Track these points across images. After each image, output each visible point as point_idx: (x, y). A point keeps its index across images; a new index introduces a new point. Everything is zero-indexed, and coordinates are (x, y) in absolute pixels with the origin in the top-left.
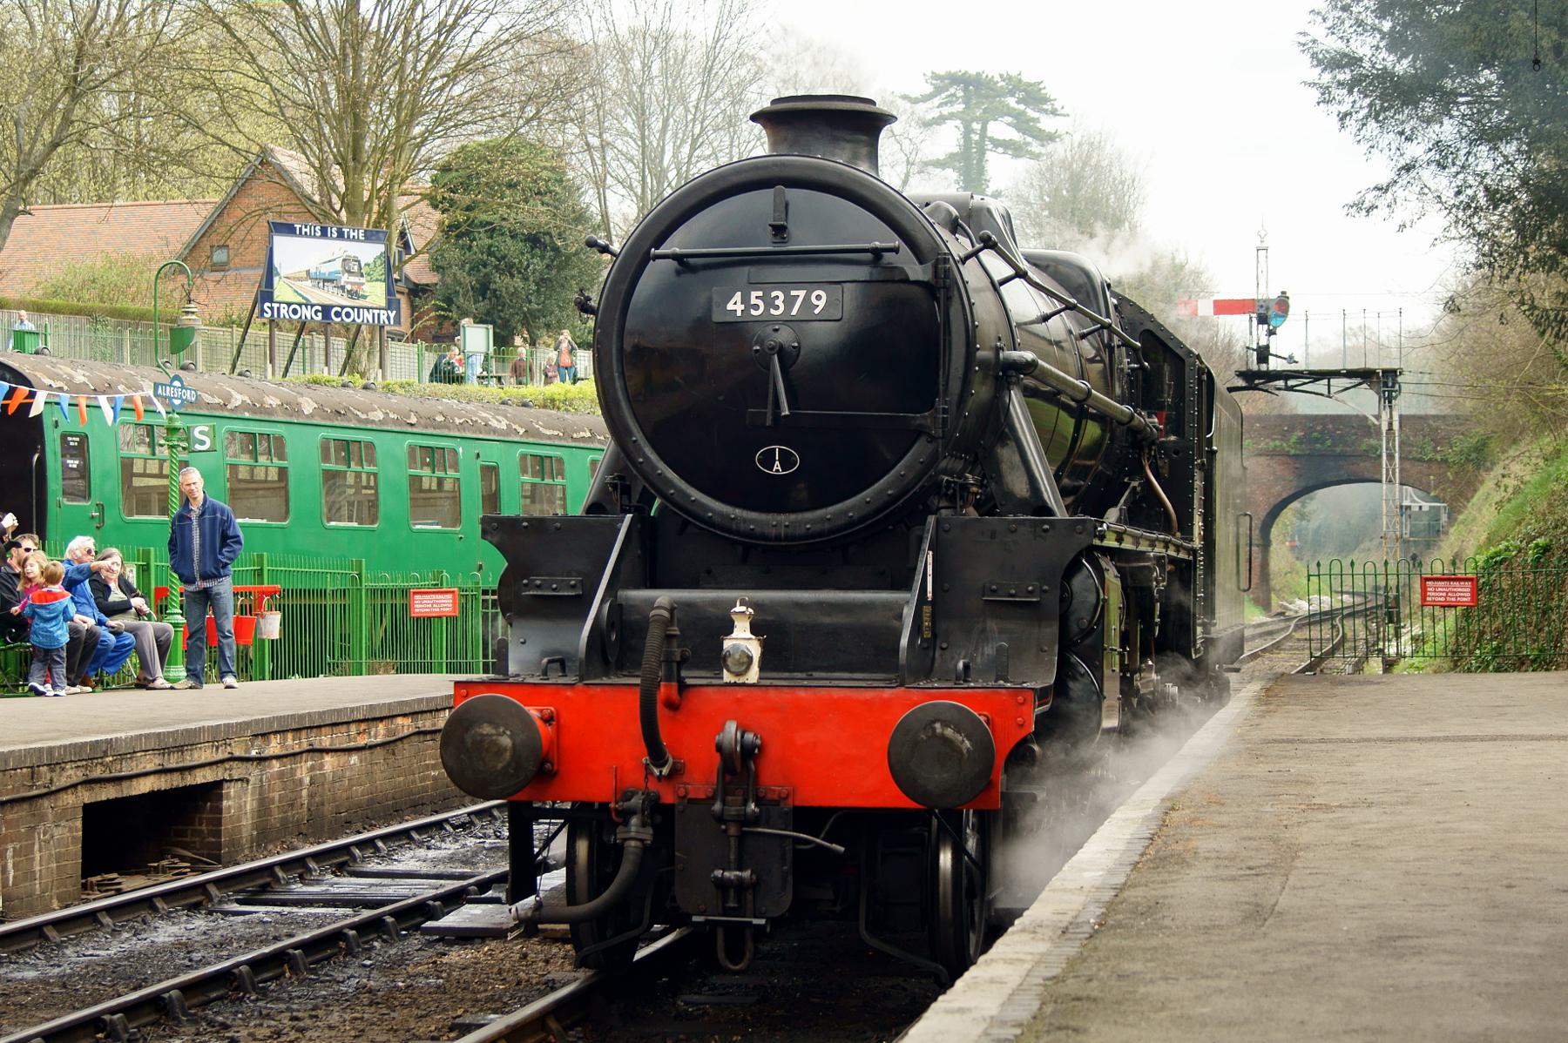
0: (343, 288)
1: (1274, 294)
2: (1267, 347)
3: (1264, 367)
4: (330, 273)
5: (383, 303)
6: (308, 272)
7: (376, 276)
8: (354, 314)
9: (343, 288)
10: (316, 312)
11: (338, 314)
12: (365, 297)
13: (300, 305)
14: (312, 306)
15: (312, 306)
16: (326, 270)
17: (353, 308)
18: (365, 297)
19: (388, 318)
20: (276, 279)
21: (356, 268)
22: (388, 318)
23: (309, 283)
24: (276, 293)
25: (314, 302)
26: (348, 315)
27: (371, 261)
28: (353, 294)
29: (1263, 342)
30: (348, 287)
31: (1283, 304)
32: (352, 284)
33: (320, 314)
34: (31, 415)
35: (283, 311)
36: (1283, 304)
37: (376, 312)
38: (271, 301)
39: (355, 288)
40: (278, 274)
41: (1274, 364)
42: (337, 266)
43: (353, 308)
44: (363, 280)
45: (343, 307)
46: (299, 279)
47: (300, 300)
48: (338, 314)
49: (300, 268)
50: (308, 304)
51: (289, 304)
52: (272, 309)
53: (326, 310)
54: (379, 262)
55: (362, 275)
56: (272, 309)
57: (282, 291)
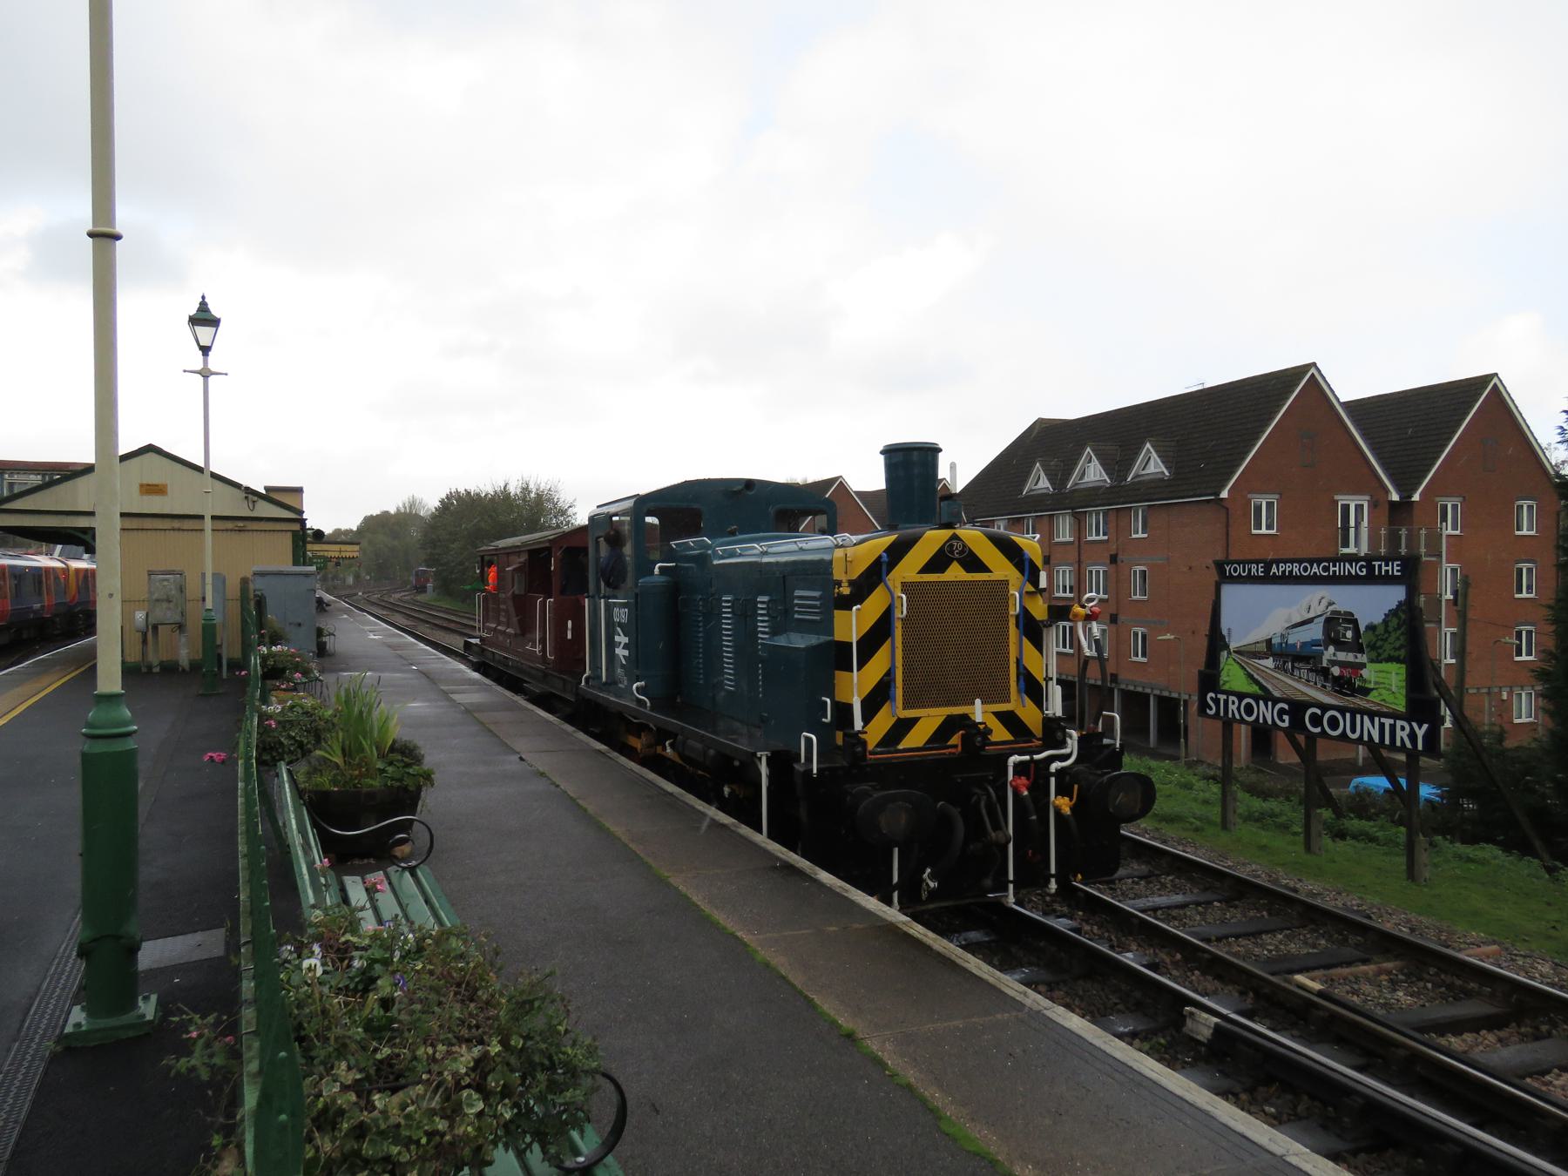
0: (1325, 672)
4: (1304, 644)
6: (1269, 642)
7: (1388, 649)
8: (1345, 723)
9: (1325, 672)
10: (1281, 712)
11: (1316, 721)
13: (1257, 698)
14: (1276, 701)
15: (1276, 701)
16: (1298, 637)
17: (1343, 711)
18: (1365, 692)
19: (1413, 736)
21: (1349, 634)
22: (1413, 736)
23: (1269, 663)
24: (1224, 677)
25: (1277, 694)
26: (1334, 723)
27: (1378, 619)
30: (1336, 671)
32: (1343, 665)
33: (1286, 717)
34: (727, 796)
35: (1233, 708)
37: (1388, 722)
39: (1346, 673)
40: (1227, 647)
42: (1316, 632)
43: (1343, 711)
44: (1362, 658)
45: (1325, 708)
47: (1255, 689)
50: (1267, 697)
51: (1241, 696)
52: (1216, 701)
53: (1297, 708)
54: (1394, 622)
55: (1361, 651)
56: (1216, 701)
57: (1233, 676)
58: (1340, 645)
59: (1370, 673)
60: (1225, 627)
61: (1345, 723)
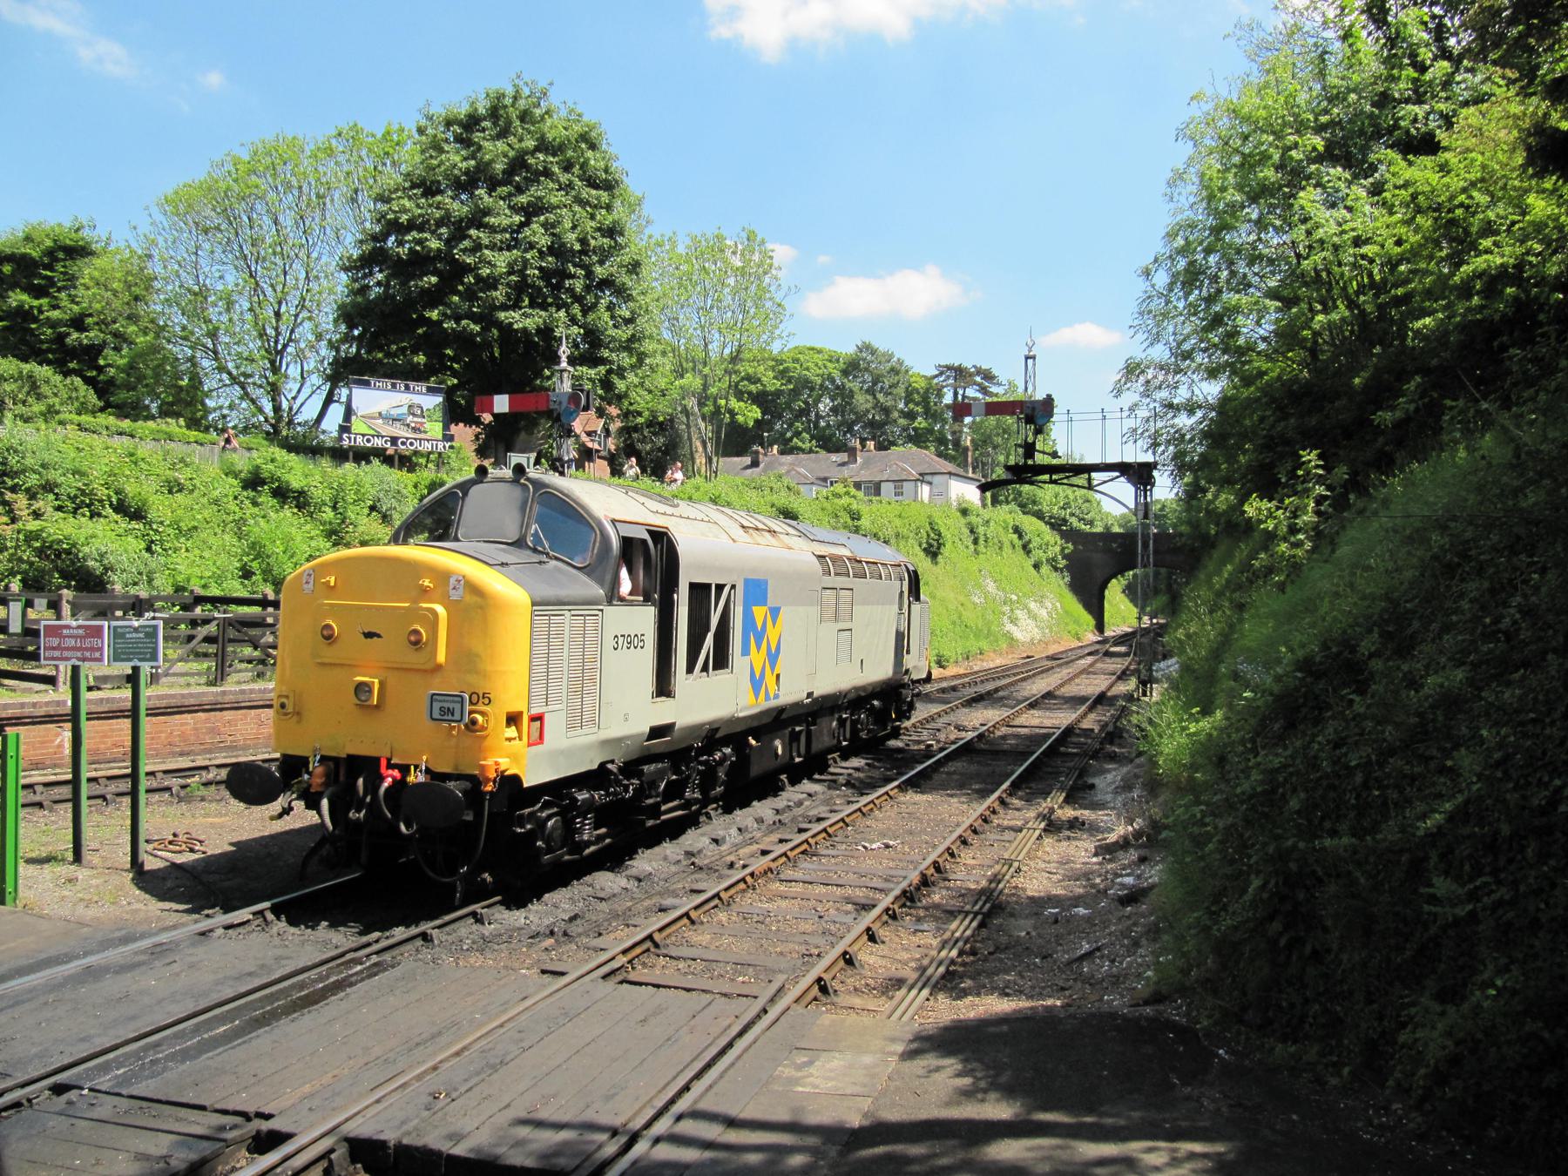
0: (408, 425)
1: (1040, 396)
2: (1034, 443)
3: (1030, 462)
5: (440, 437)
6: (380, 414)
8: (416, 444)
9: (408, 425)
12: (425, 432)
16: (395, 412)
18: (425, 432)
20: (353, 418)
23: (380, 421)
26: (411, 444)
28: (415, 430)
29: (1030, 439)
31: (1048, 404)
36: (1048, 404)
38: (349, 432)
41: (1040, 459)
42: (405, 410)
46: (374, 418)
47: (372, 432)
48: (403, 443)
49: (375, 410)
51: (364, 435)
52: (350, 438)
53: (394, 440)
56: (350, 438)
57: (358, 426)
58: (414, 415)
59: (428, 426)
60: (354, 406)
61: (416, 444)
